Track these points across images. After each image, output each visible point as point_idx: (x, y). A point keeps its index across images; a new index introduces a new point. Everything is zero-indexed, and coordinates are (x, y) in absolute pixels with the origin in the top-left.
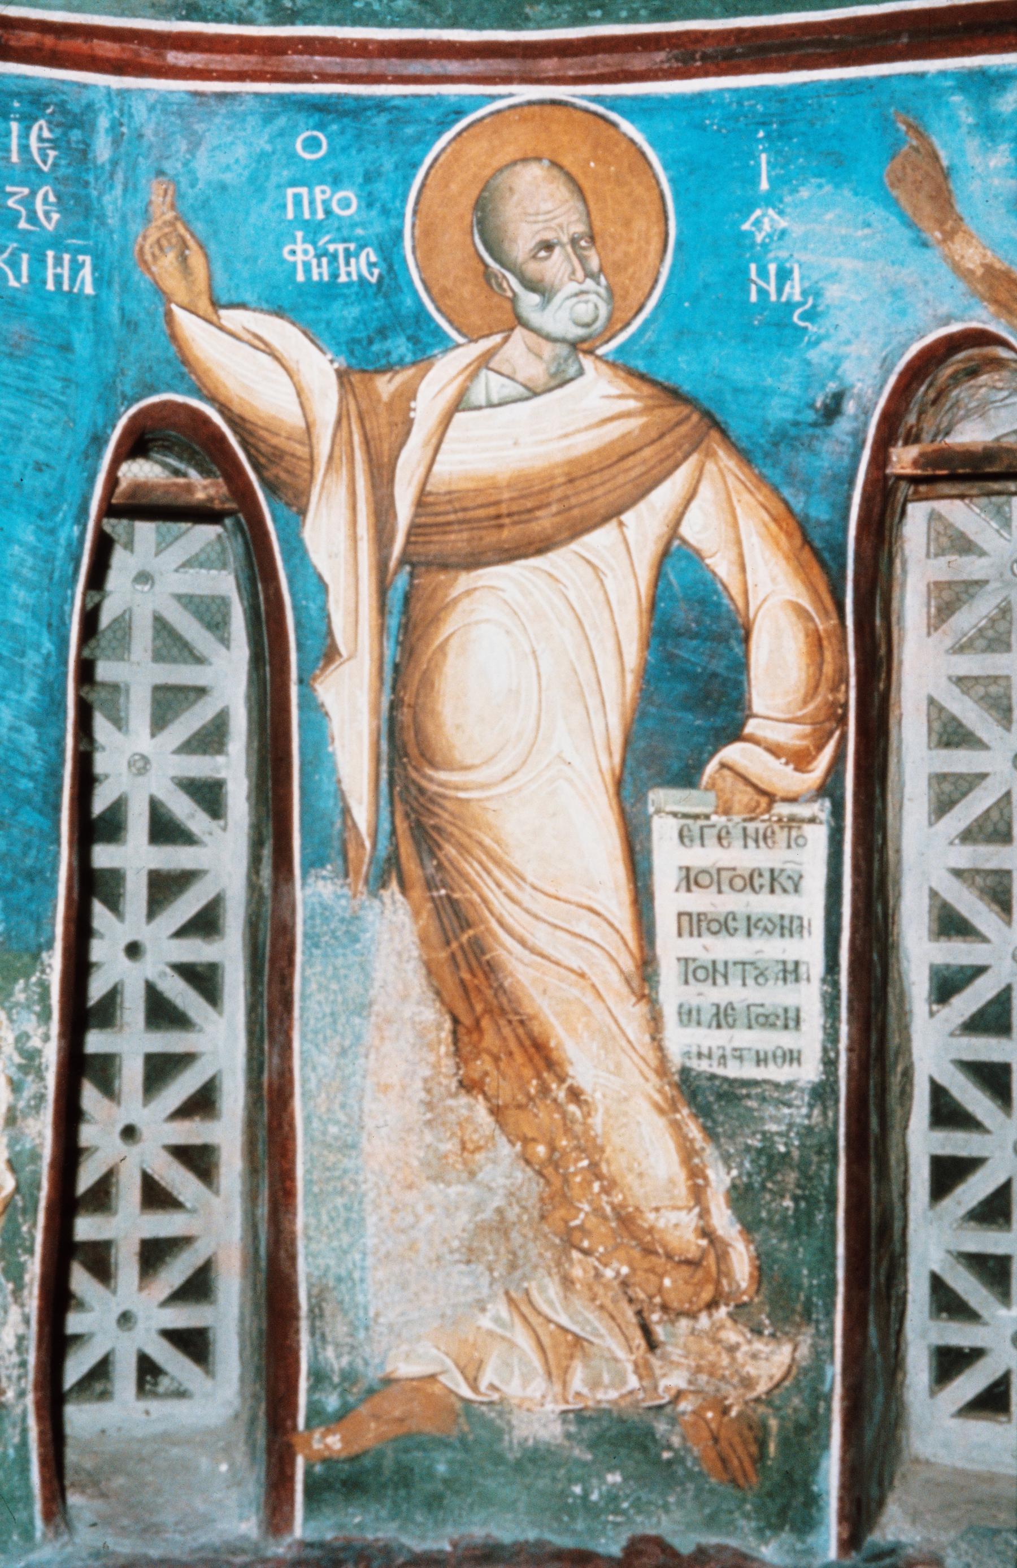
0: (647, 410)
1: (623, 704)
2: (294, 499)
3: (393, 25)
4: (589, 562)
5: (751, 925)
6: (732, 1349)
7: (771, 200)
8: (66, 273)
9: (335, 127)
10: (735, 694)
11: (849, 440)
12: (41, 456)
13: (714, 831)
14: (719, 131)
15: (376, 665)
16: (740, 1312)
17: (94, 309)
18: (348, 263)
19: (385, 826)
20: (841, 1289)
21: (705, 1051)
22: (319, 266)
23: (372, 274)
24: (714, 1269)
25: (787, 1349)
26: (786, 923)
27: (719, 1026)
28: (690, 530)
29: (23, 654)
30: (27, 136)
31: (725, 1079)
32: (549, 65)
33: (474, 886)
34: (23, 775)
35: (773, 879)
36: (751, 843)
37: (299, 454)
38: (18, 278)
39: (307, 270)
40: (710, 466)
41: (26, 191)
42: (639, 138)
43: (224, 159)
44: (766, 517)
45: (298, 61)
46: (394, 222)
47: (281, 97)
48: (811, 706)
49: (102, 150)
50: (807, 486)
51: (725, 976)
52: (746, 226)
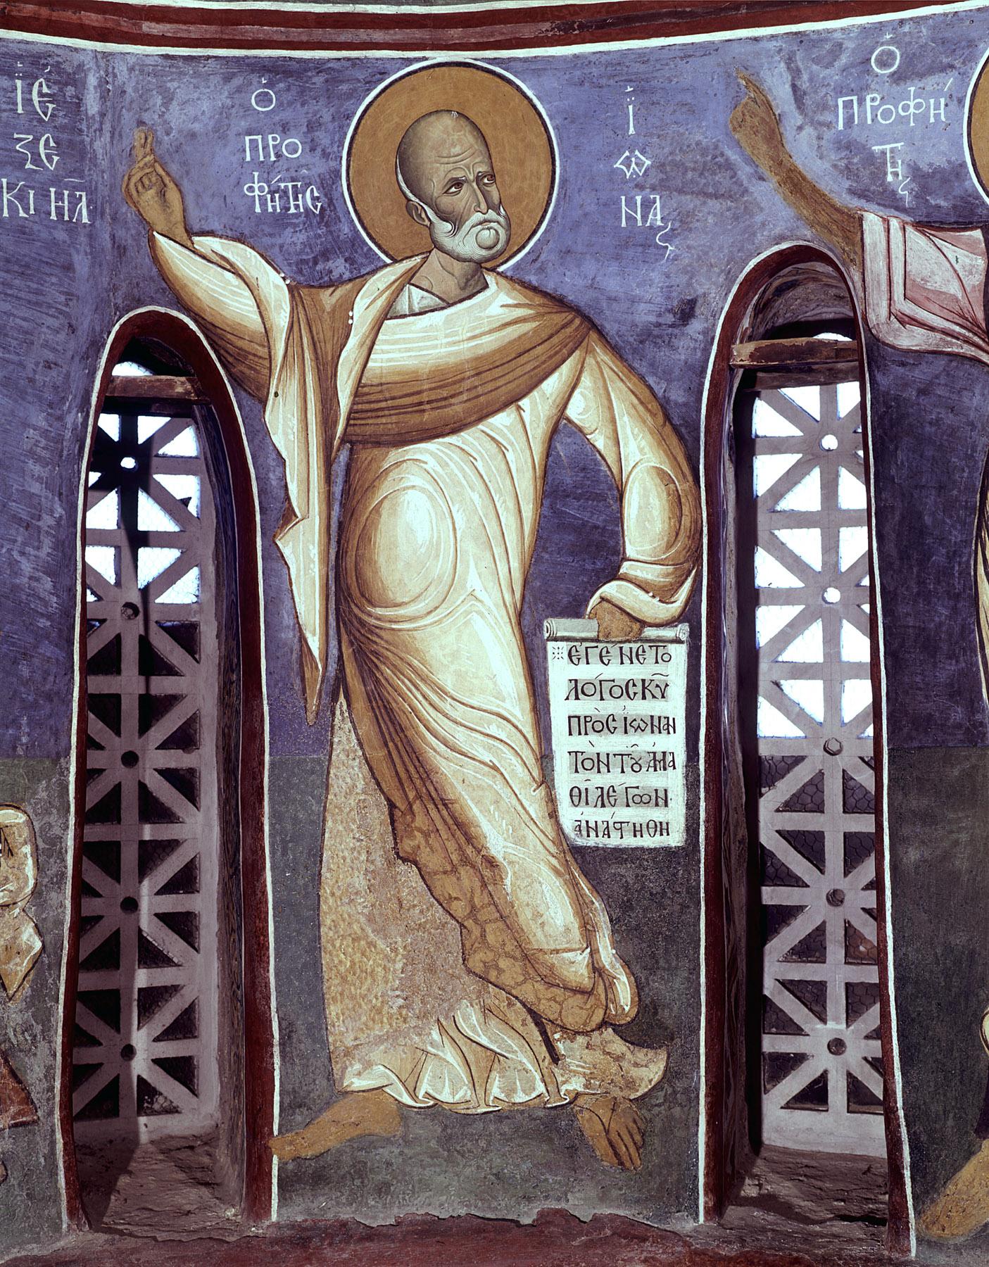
1: (523, 553)
4: (493, 439)
5: (629, 725)
6: (619, 1058)
9: (282, 85)
12: (51, 356)
15: (324, 522)
17: (91, 237)
18: (296, 199)
19: (334, 652)
20: (703, 1009)
23: (316, 207)
24: (603, 996)
26: (656, 723)
27: (603, 805)
28: (575, 411)
32: (455, 34)
34: (42, 615)
35: (644, 688)
36: (626, 660)
37: (260, 354)
38: (26, 210)
39: (263, 203)
40: (590, 361)
41: (31, 137)
42: (530, 93)
43: (191, 111)
44: (636, 401)
45: (251, 31)
46: (332, 164)
47: (237, 60)
49: (92, 104)
50: (667, 376)
51: (608, 766)
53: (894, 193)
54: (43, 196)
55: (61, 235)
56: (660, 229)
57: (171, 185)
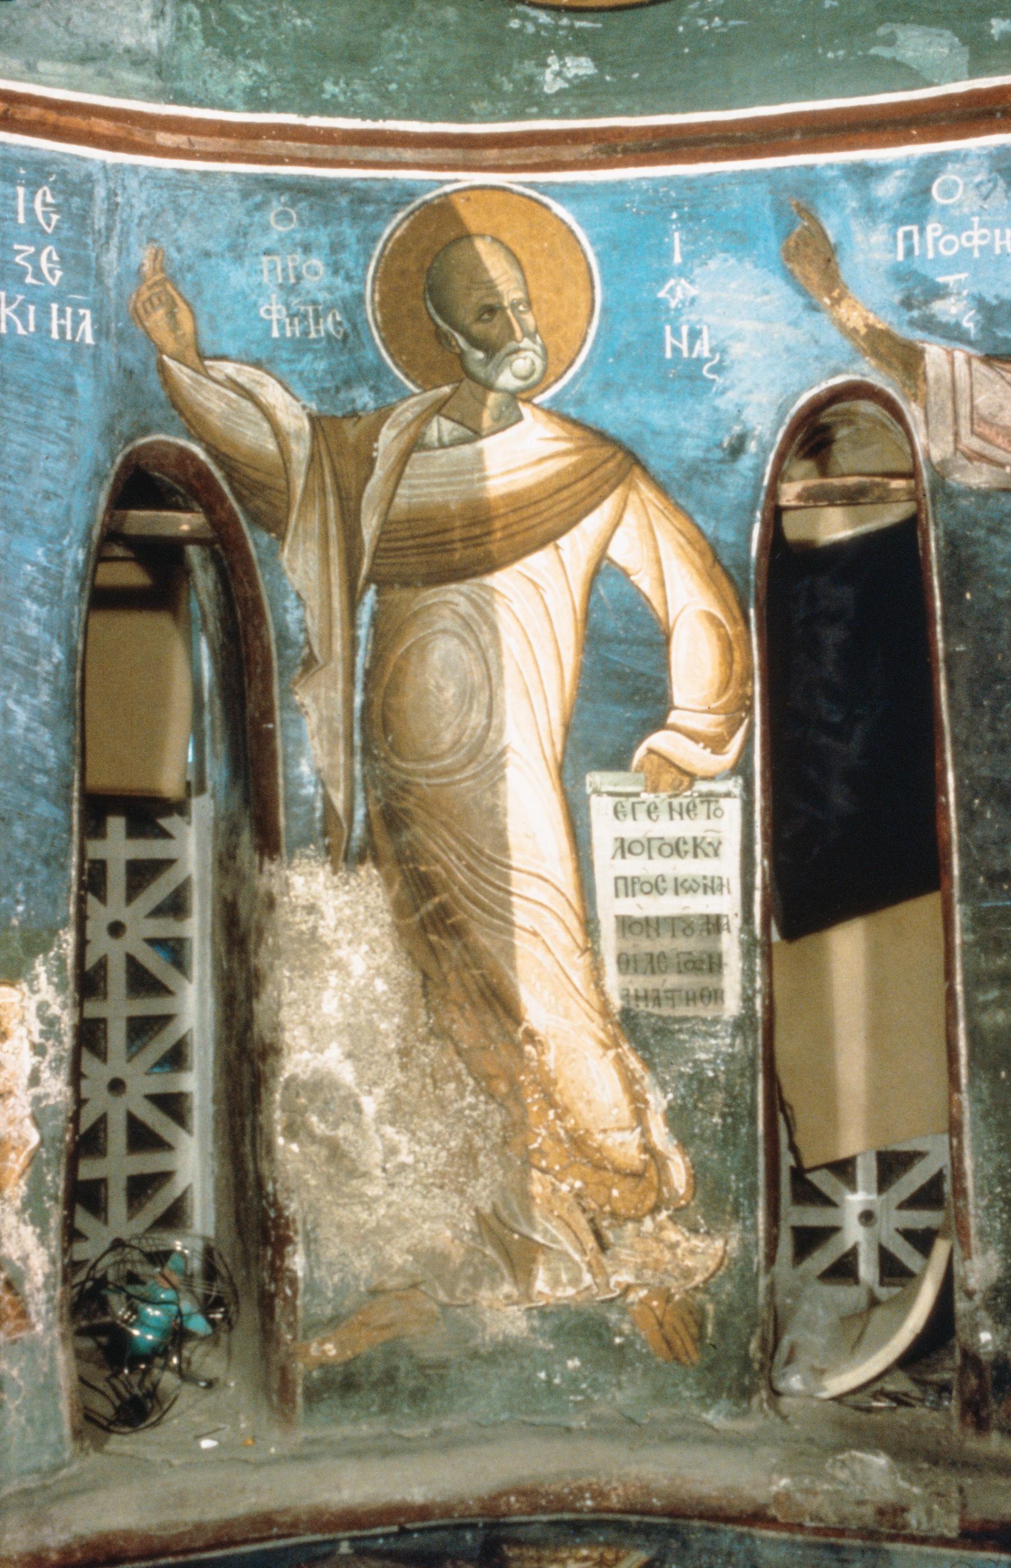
0: (578, 450)
1: (563, 701)
2: (275, 525)
3: (355, 115)
5: (682, 886)
6: (673, 1246)
7: (682, 272)
8: (69, 324)
10: (659, 690)
11: (751, 474)
12: (49, 485)
13: (644, 807)
14: (638, 213)
16: (679, 1216)
18: (317, 323)
21: (641, 993)
22: (291, 324)
24: (655, 1179)
25: (719, 1243)
27: (653, 972)
28: (617, 552)
29: (36, 663)
30: (33, 201)
31: (660, 1017)
33: (438, 860)
34: (39, 771)
35: (696, 846)
36: (676, 816)
38: (26, 327)
39: (282, 327)
40: (633, 497)
41: (32, 250)
44: (682, 540)
46: (356, 287)
48: (725, 698)
50: (715, 513)
52: (662, 294)
53: (958, 325)
54: (44, 313)
55: (63, 356)
56: (707, 360)
57: (181, 305)
